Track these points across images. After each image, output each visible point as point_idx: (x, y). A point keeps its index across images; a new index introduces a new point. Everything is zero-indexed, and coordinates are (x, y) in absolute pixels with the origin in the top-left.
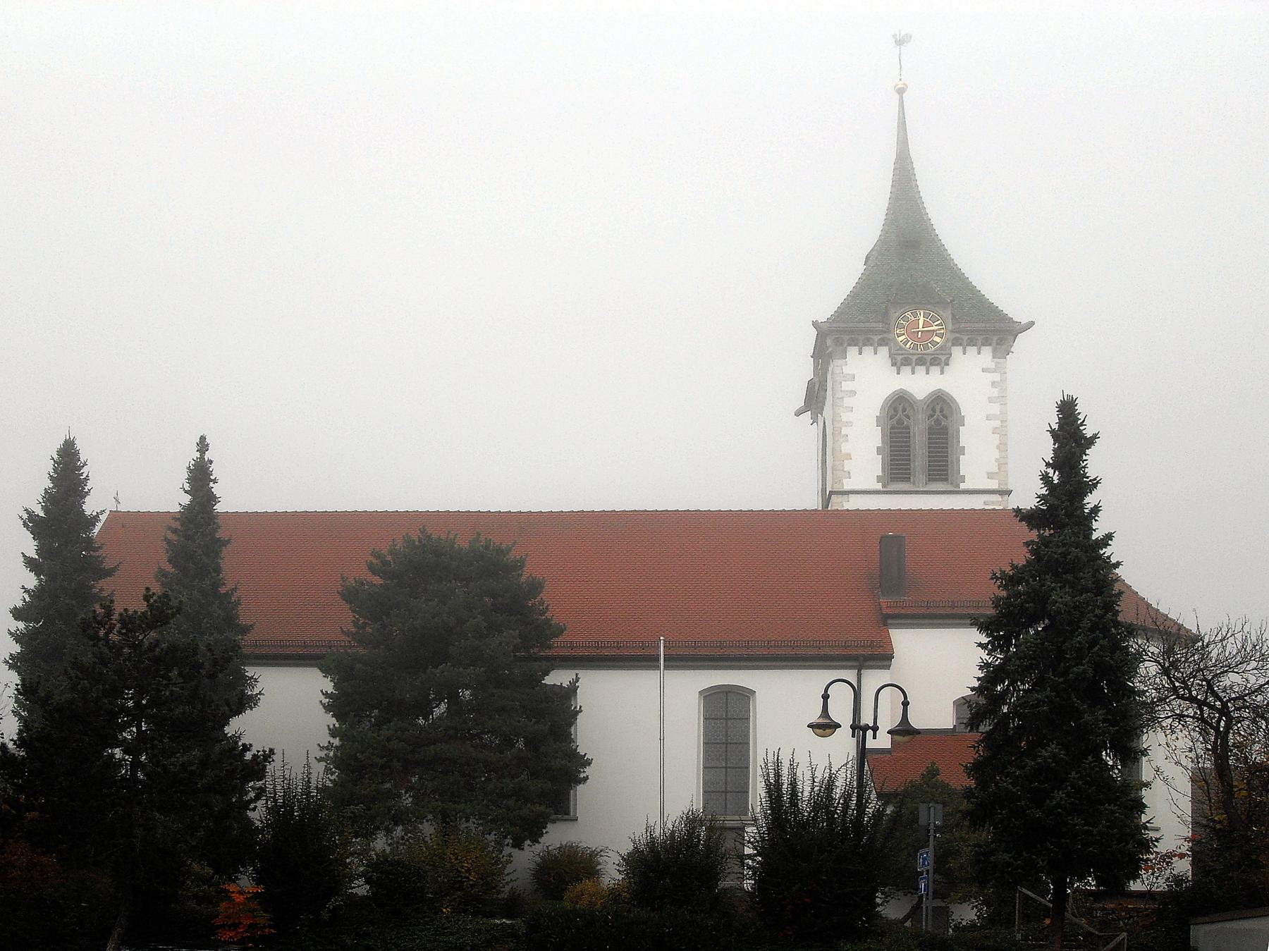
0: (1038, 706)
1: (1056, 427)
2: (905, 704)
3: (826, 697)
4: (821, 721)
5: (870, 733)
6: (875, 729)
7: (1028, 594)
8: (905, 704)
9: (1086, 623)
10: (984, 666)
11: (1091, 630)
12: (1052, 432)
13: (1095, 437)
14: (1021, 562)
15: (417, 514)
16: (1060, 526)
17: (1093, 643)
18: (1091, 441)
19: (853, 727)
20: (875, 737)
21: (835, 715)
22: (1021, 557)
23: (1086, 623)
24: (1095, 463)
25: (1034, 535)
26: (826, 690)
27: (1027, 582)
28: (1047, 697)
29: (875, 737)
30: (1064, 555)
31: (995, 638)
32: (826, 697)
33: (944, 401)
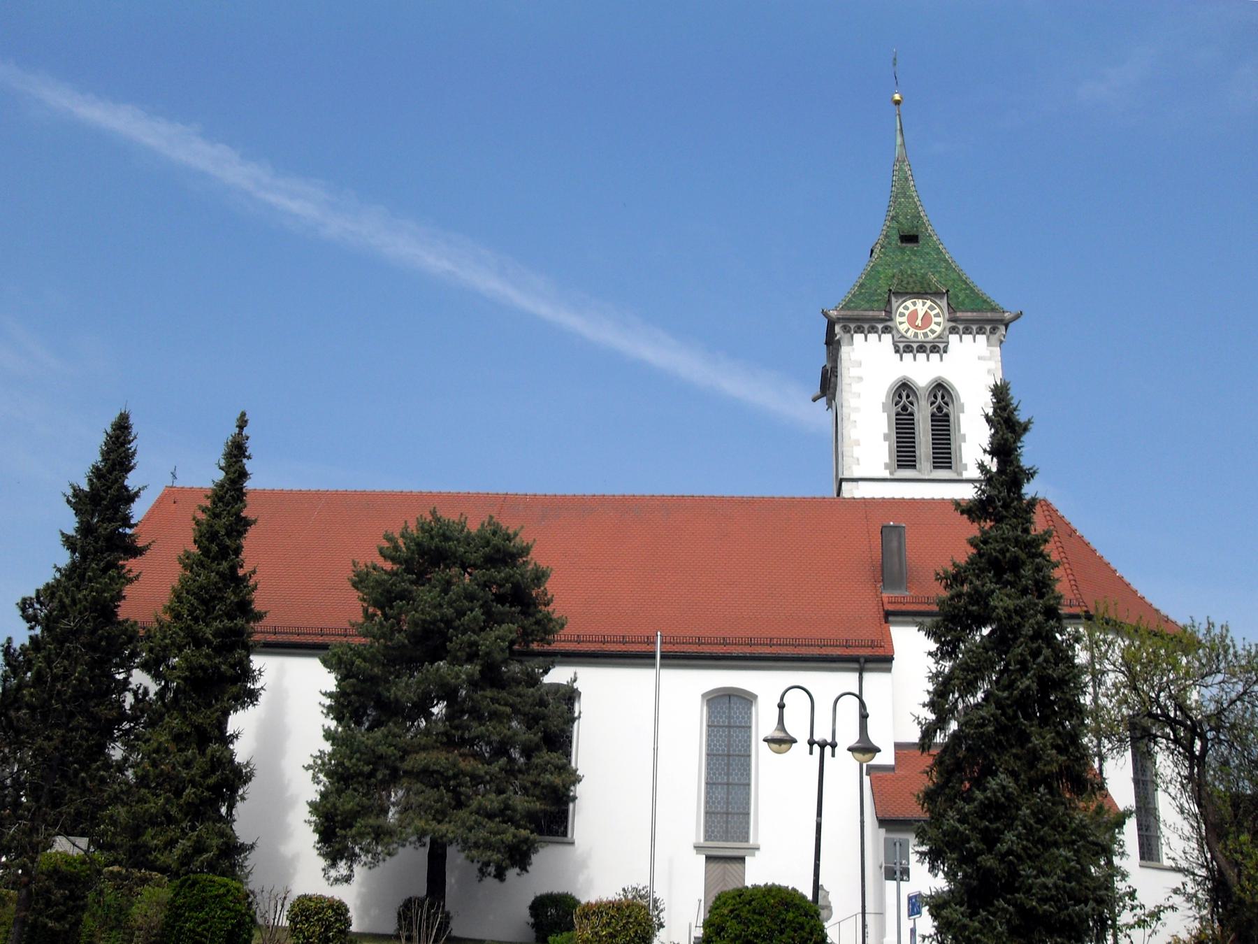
0: (983, 725)
1: (990, 412)
2: (864, 717)
3: (781, 706)
4: (780, 735)
5: (828, 749)
6: (834, 746)
7: (969, 595)
8: (864, 717)
9: (1027, 630)
10: (934, 677)
11: (1033, 638)
12: (987, 416)
13: (1029, 422)
14: (962, 559)
15: (363, 494)
16: (999, 519)
17: (1036, 654)
18: (1025, 428)
19: (811, 743)
20: (833, 755)
21: (792, 730)
22: (963, 554)
23: (1027, 630)
24: (1029, 453)
25: (974, 530)
26: (782, 699)
27: (971, 583)
28: (992, 715)
29: (833, 755)
30: (1003, 552)
31: (943, 644)
32: (781, 706)
33: (910, 388)
